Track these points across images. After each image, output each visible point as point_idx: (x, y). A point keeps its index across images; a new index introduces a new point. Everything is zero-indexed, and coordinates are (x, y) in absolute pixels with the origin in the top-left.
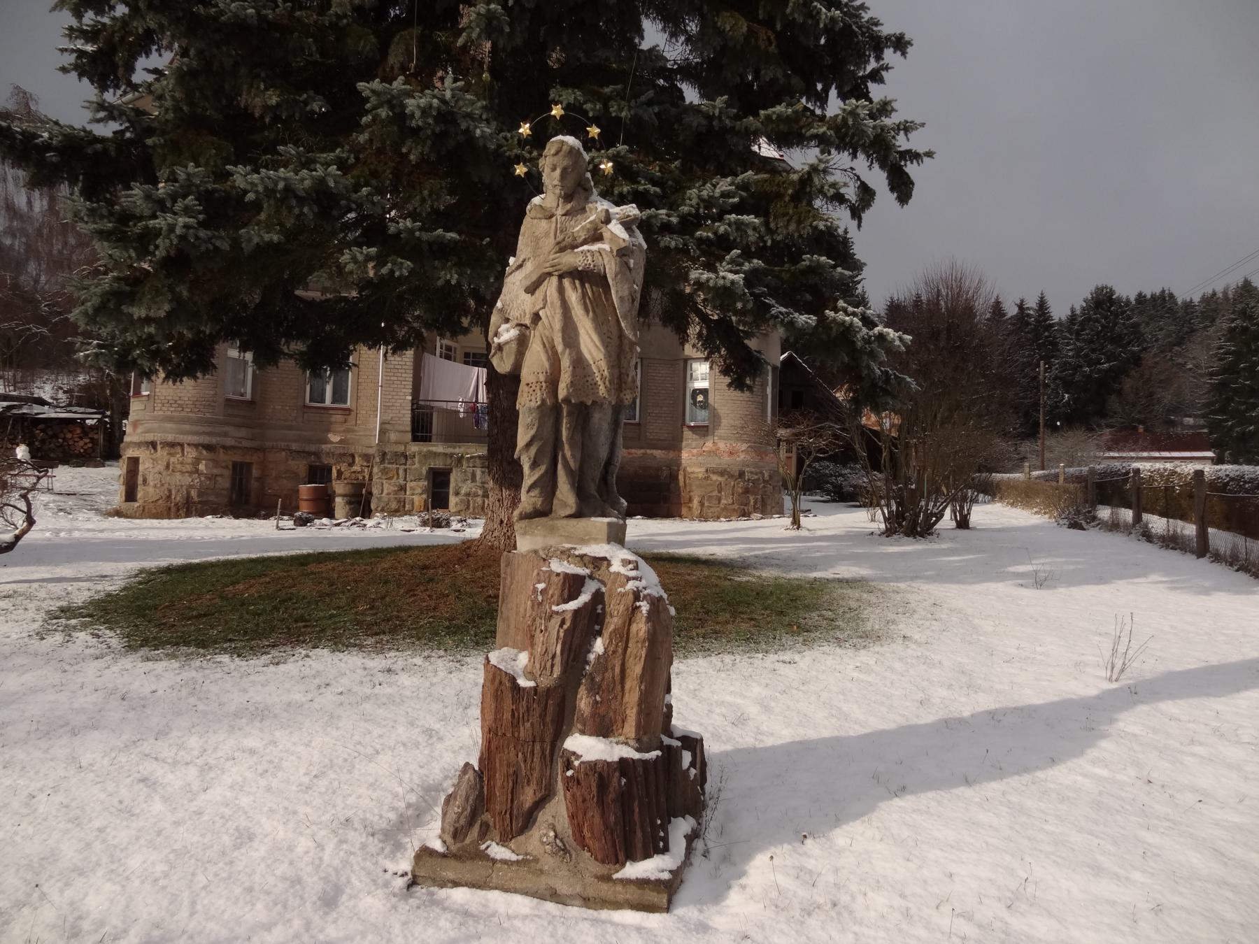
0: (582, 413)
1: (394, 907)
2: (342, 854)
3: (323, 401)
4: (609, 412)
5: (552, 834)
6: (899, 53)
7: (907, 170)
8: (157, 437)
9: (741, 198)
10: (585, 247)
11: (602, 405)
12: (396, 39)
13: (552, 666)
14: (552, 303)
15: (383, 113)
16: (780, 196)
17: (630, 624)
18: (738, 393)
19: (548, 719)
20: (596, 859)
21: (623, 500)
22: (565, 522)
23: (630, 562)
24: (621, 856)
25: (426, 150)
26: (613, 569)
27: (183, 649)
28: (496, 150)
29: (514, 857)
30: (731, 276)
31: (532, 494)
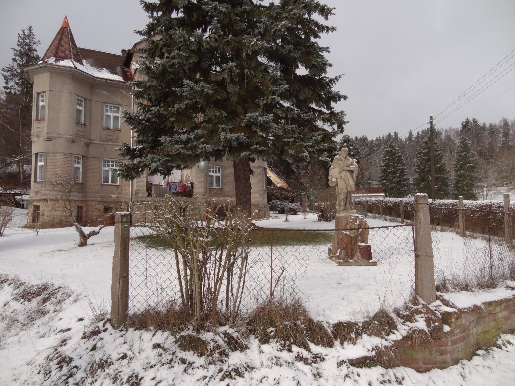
3: (108, 182)
8: (48, 197)
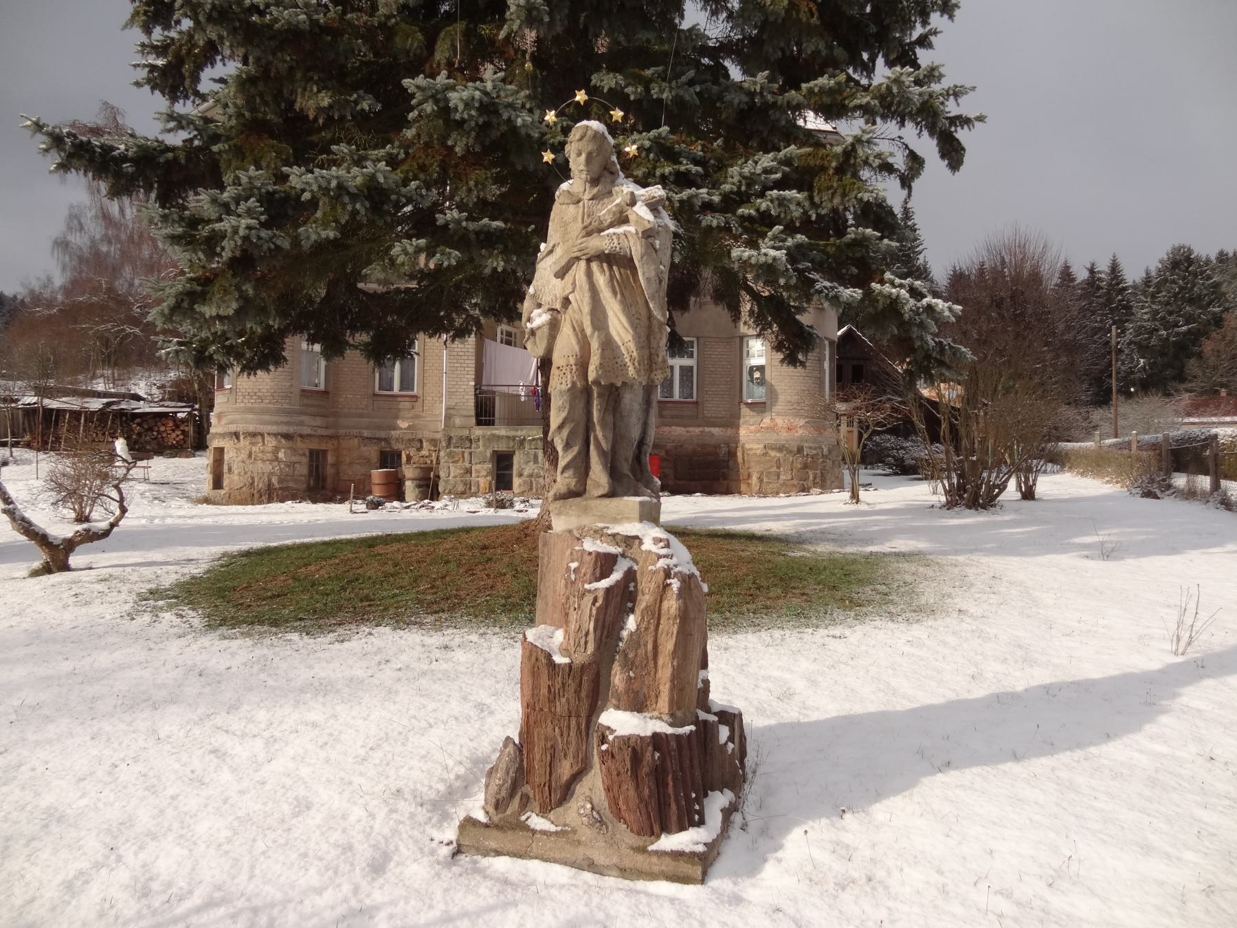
0: (613, 394)
1: (438, 875)
2: (391, 823)
3: (391, 389)
4: (640, 393)
5: (589, 806)
6: (946, 16)
7: (957, 136)
8: (240, 428)
10: (611, 231)
12: (442, 35)
13: (586, 643)
15: (429, 107)
16: (823, 169)
17: (661, 602)
18: (791, 368)
19: (583, 694)
20: (632, 831)
21: (656, 479)
22: (598, 502)
23: (661, 540)
24: (656, 828)
25: (471, 141)
26: (644, 548)
27: (258, 628)
28: (540, 138)
29: (553, 828)
30: (772, 253)
31: (566, 475)
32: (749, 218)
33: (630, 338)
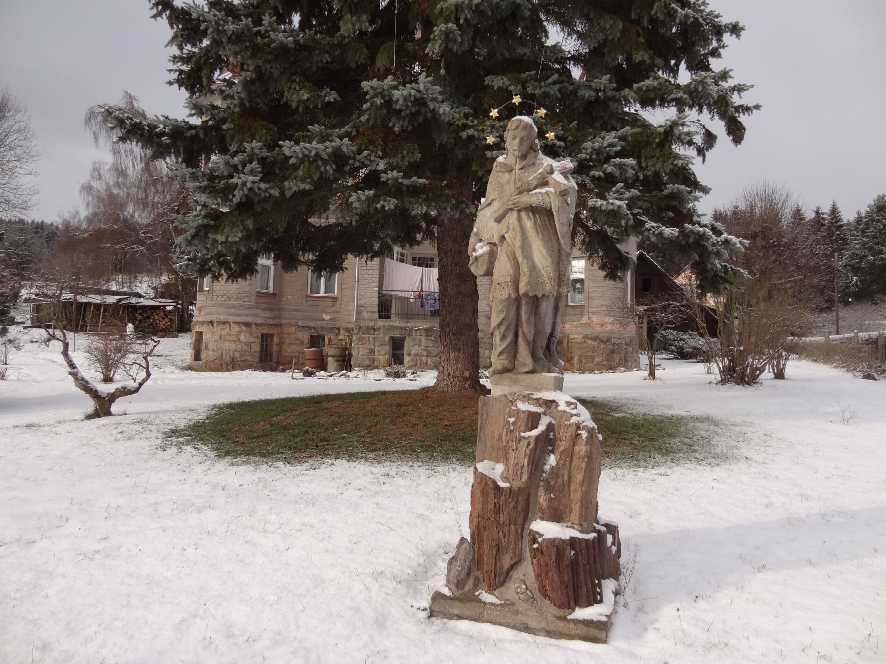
0: (535, 302)
1: (424, 631)
2: (383, 594)
3: (319, 292)
5: (524, 587)
6: (734, 36)
7: (740, 119)
9: (622, 146)
10: (537, 191)
11: (548, 297)
12: (381, 50)
13: (522, 473)
14: (514, 229)
15: (378, 101)
16: (649, 143)
17: (574, 446)
18: (612, 282)
19: (520, 509)
20: (555, 605)
21: (561, 361)
22: (525, 376)
23: (572, 404)
24: (572, 604)
25: (406, 124)
26: (560, 408)
27: (253, 458)
28: (449, 121)
29: (498, 602)
30: (618, 202)
32: (599, 177)
33: (549, 264)
